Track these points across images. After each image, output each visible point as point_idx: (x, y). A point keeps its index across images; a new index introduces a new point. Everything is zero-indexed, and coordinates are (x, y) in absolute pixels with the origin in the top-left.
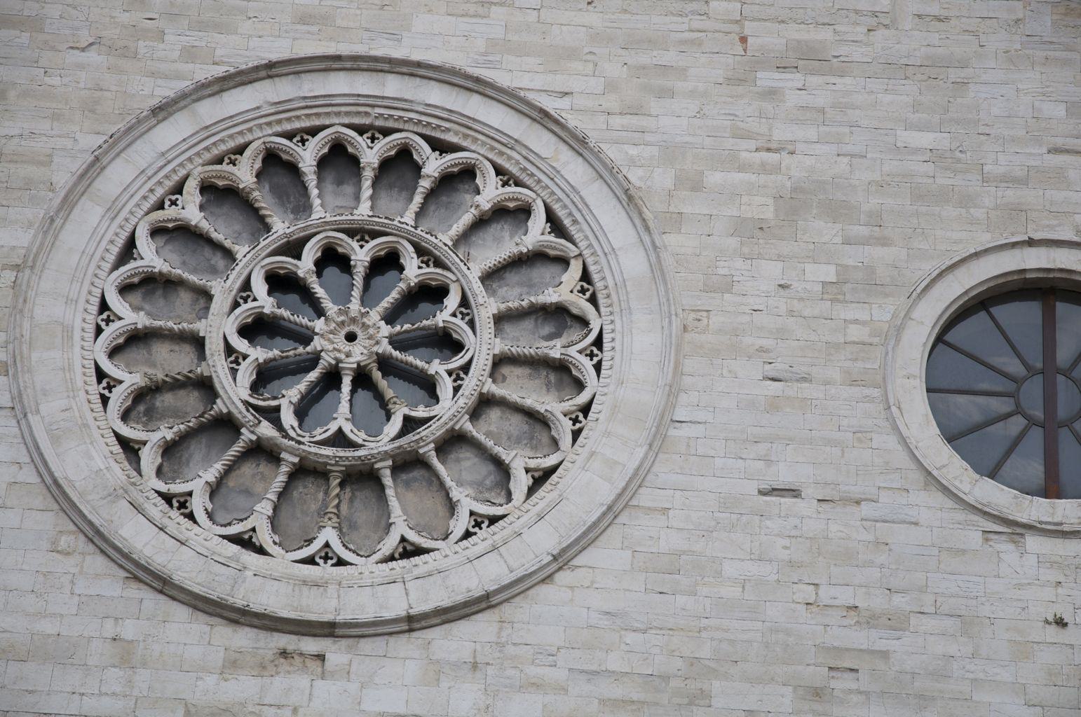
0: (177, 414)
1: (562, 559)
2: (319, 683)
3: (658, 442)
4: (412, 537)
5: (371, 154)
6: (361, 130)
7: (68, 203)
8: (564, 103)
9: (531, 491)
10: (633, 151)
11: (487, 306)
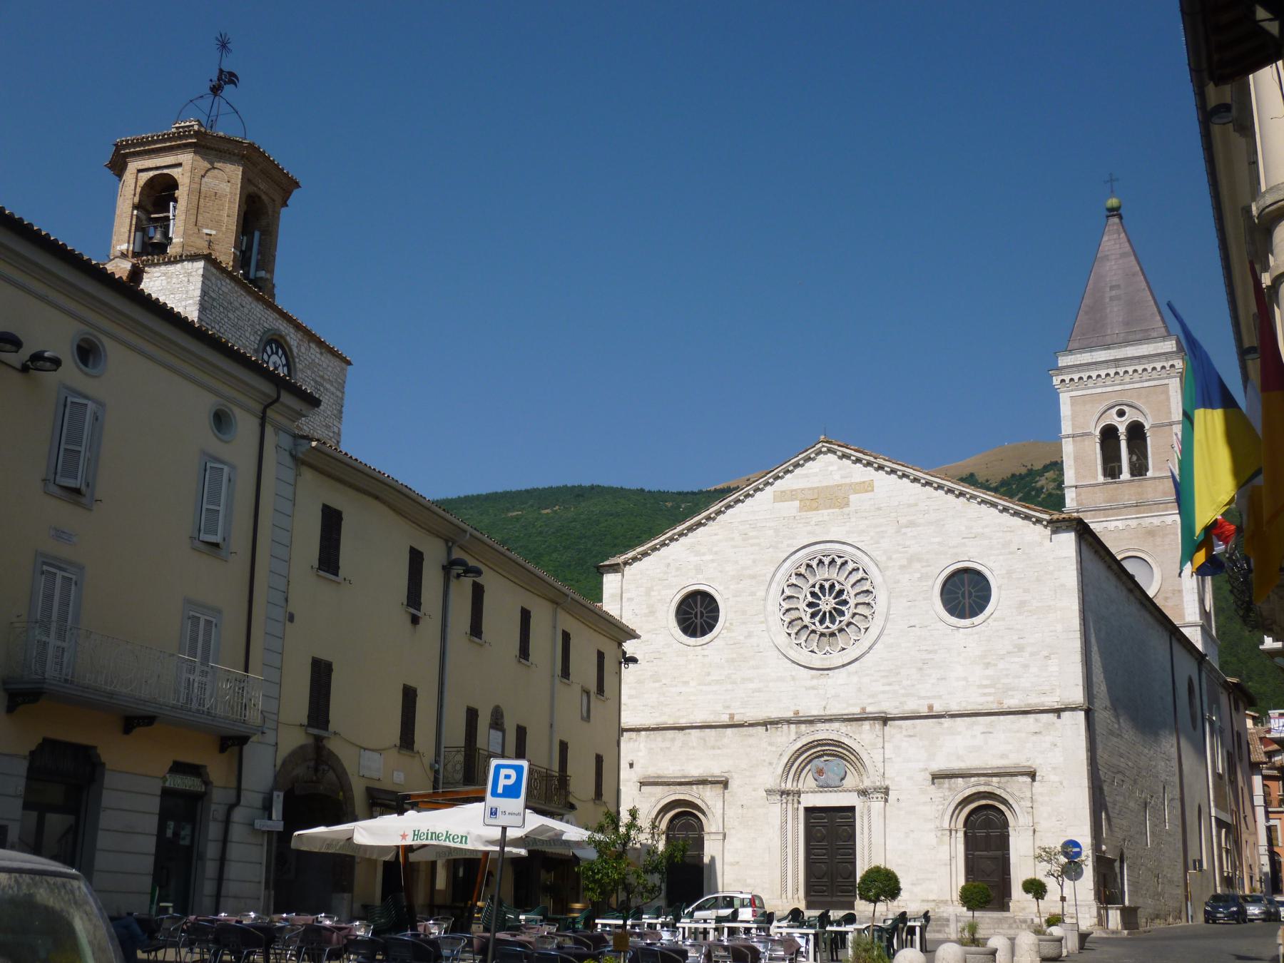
0: (798, 625)
1: (870, 648)
2: (829, 680)
3: (886, 620)
4: (843, 646)
5: (826, 561)
6: (824, 556)
7: (770, 585)
8: (863, 543)
9: (865, 632)
10: (878, 553)
11: (852, 593)
